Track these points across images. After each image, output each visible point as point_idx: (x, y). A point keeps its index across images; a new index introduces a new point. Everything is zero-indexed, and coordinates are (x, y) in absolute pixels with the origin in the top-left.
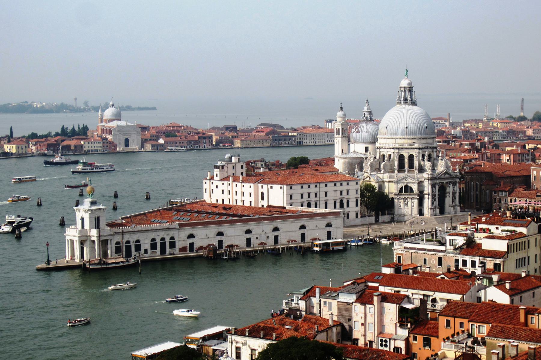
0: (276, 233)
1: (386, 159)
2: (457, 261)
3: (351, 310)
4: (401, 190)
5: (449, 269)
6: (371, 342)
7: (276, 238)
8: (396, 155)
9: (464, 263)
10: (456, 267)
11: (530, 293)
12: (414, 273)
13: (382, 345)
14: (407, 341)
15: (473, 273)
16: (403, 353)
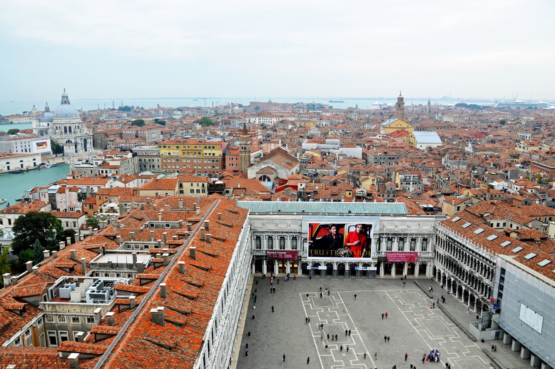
0: (8, 165)
1: (58, 128)
2: (99, 171)
3: (55, 196)
4: (66, 142)
5: (96, 175)
6: (66, 210)
7: (8, 167)
8: (63, 127)
9: (102, 172)
10: (99, 174)
11: (132, 182)
12: (81, 177)
13: (71, 210)
14: (82, 207)
15: (107, 176)
16: (81, 212)
